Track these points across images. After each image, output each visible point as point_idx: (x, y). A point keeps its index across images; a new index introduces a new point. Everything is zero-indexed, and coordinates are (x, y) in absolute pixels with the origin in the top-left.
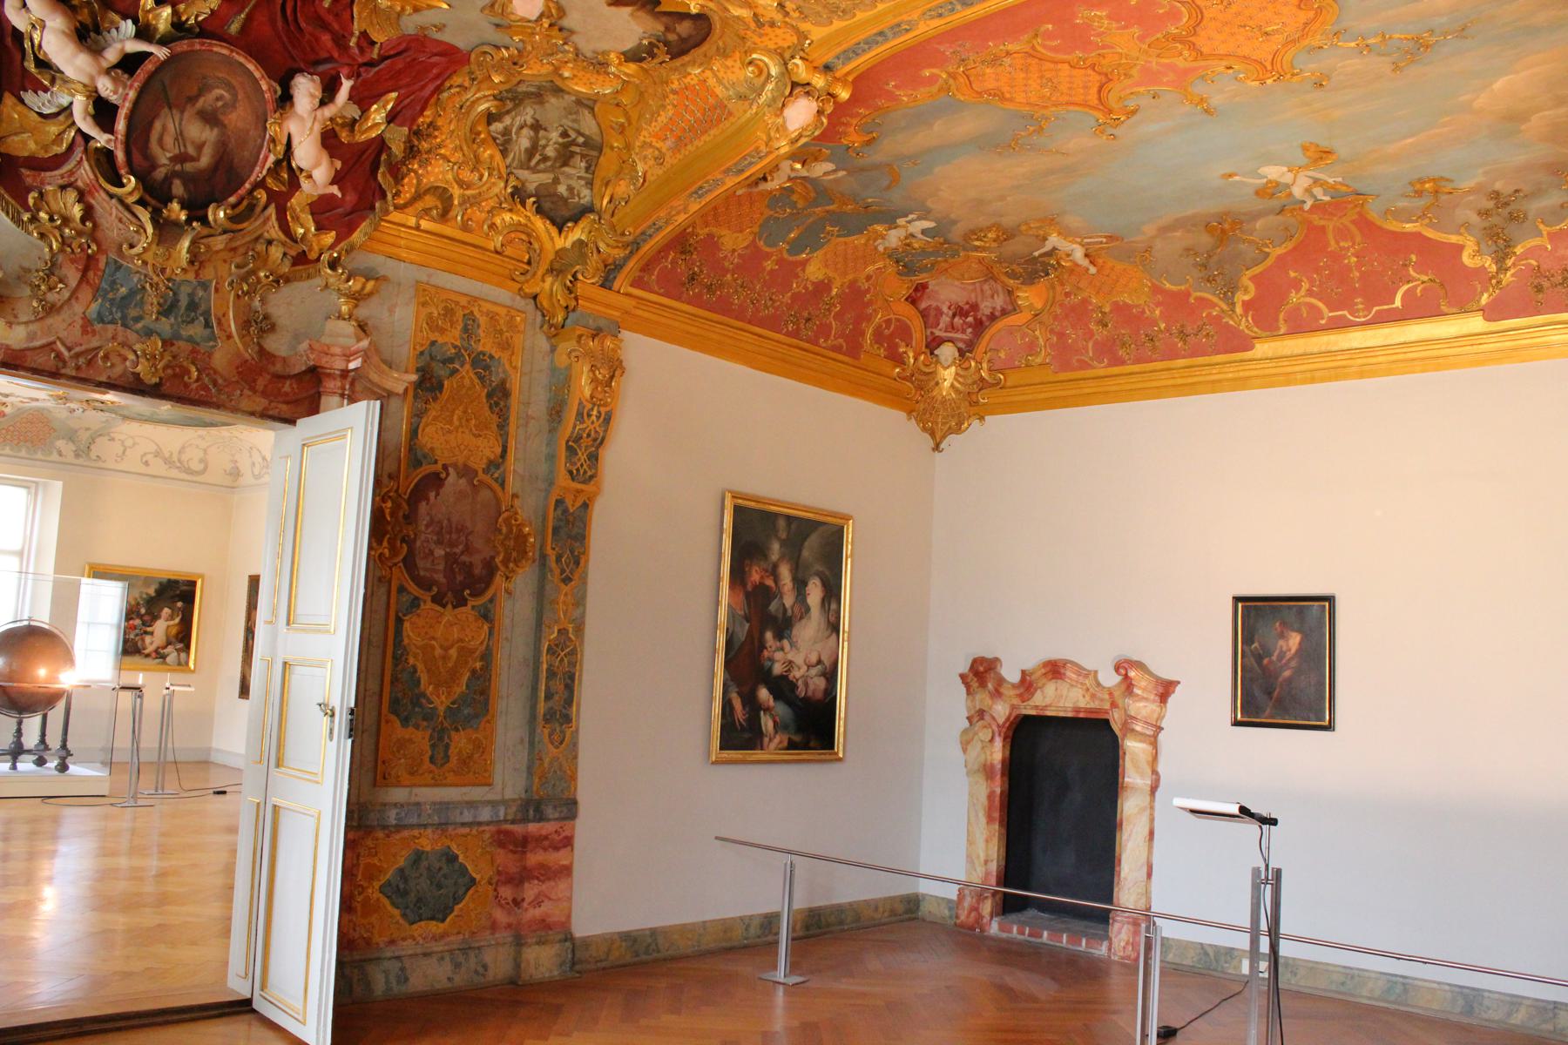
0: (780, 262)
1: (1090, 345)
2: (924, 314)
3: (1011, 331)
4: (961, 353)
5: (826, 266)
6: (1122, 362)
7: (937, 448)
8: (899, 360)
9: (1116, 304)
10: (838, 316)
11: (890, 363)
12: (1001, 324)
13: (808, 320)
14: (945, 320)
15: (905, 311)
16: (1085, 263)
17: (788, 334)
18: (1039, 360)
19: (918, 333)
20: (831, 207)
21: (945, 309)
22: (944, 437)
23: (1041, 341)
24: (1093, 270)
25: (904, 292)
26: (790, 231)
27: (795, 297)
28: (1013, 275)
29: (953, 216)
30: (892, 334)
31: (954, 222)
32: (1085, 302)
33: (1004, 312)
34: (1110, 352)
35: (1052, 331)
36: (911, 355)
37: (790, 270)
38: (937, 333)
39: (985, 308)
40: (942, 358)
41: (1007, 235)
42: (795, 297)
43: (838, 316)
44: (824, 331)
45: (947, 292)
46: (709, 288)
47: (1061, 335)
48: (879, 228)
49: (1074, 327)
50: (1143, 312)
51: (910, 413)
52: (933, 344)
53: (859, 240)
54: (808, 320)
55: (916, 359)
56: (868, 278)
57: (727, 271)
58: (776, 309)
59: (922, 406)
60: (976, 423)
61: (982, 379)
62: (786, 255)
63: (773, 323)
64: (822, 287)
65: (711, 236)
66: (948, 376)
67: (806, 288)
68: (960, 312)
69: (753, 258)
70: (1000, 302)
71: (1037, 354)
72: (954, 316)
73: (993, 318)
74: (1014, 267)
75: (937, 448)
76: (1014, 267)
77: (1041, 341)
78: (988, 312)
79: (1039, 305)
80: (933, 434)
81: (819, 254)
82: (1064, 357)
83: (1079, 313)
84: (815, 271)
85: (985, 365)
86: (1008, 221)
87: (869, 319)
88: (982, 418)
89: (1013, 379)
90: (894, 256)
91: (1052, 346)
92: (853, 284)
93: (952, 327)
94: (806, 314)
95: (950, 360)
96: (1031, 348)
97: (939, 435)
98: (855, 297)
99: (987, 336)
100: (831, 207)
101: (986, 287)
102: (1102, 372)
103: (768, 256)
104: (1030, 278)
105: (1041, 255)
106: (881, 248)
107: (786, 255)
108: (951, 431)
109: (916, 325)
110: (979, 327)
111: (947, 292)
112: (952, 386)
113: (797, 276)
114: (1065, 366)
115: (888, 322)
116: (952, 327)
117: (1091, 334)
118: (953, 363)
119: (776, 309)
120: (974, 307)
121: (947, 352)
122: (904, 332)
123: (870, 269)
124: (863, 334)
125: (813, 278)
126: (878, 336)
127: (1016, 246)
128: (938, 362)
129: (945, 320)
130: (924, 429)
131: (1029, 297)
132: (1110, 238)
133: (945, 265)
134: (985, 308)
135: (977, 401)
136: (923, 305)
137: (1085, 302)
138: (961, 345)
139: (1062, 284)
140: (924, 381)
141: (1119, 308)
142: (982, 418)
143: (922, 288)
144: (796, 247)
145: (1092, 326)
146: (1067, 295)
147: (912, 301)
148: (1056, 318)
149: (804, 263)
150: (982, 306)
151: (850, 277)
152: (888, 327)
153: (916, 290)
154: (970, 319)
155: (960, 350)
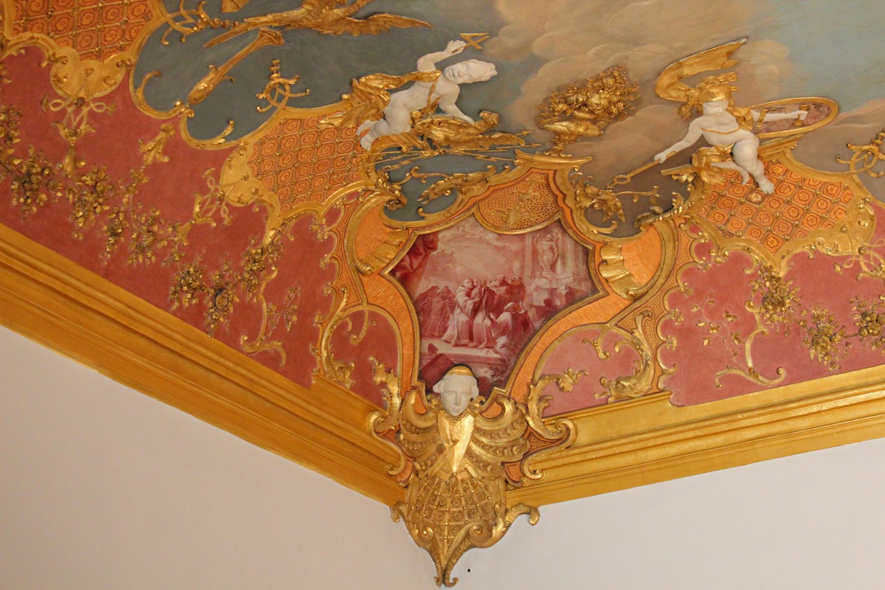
0: (173, 147)
1: (748, 346)
2: (421, 306)
3: (585, 337)
4: (484, 387)
5: (260, 175)
6: (819, 372)
7: (443, 578)
8: (374, 396)
9: (800, 258)
10: (274, 292)
11: (360, 402)
12: (562, 324)
13: (220, 290)
14: (459, 318)
15: (387, 299)
16: (757, 169)
17: (181, 314)
18: (644, 385)
19: (408, 349)
20: (296, 13)
21: (461, 297)
22: (456, 555)
23: (647, 352)
24: (767, 186)
25: (392, 255)
26: (200, 75)
27: (197, 234)
28: (596, 216)
29: (538, 46)
30: (363, 345)
31: (534, 64)
32: (738, 260)
33: (573, 298)
34: (795, 355)
35: (667, 327)
36: (395, 389)
37: (193, 168)
38: (443, 348)
39: (536, 293)
40: (449, 400)
41: (628, 95)
42: (197, 234)
43: (274, 292)
44: (246, 318)
45: (470, 258)
46: (25, 179)
47: (687, 333)
48: (375, 82)
49: (711, 314)
50: (857, 268)
51: (396, 505)
52: (433, 370)
53: (329, 117)
54: (220, 290)
55: (403, 401)
56: (332, 215)
57: (62, 148)
58: (160, 255)
59: (412, 494)
60: (520, 522)
61: (529, 434)
62: (184, 135)
63: (152, 285)
64: (249, 220)
65: (33, 53)
66: (462, 433)
67: (219, 220)
68: (488, 302)
69: (119, 126)
70: (566, 276)
71: (639, 374)
72: (475, 311)
73: (549, 311)
74: (608, 195)
75: (443, 578)
76: (608, 195)
77: (647, 352)
78: (539, 299)
79: (641, 278)
80: (434, 552)
81: (251, 139)
82: (698, 375)
83: (726, 284)
84: (237, 182)
85: (533, 407)
86: (640, 60)
87: (325, 305)
88: (532, 511)
89: (584, 430)
90: (388, 161)
91: (668, 357)
92: (303, 223)
93: (470, 336)
94: (215, 277)
95: (465, 401)
96: (628, 362)
97: (445, 552)
98: (304, 248)
99: (537, 347)
100: (296, 13)
101: (544, 245)
102: (776, 395)
103: (149, 129)
104: (631, 222)
105: (671, 162)
106: (367, 143)
107: (184, 135)
108: (470, 542)
109: (404, 328)
110: (522, 331)
111: (470, 258)
112: (469, 453)
113: (204, 191)
114: (697, 390)
115: (357, 317)
116: (470, 336)
117: (750, 323)
118: (470, 409)
119: (160, 255)
120: (516, 290)
121: (458, 386)
122: (383, 342)
123: (337, 196)
124: (314, 337)
125: (232, 197)
126: (339, 339)
127: (628, 140)
128: (441, 407)
129: (459, 318)
130: (421, 541)
131: (626, 264)
132: (817, 108)
133: (477, 190)
134: (536, 293)
135: (518, 478)
136: (422, 287)
137: (738, 260)
138: (485, 372)
139: (695, 229)
140: (420, 442)
141: (809, 267)
142: (532, 511)
143: (424, 245)
144: (207, 119)
145: (754, 310)
146: (703, 250)
147: (404, 276)
148: (676, 300)
149: (219, 159)
150: (530, 288)
151: (300, 208)
152: (357, 329)
153: (413, 252)
154: (505, 317)
155: (480, 381)
